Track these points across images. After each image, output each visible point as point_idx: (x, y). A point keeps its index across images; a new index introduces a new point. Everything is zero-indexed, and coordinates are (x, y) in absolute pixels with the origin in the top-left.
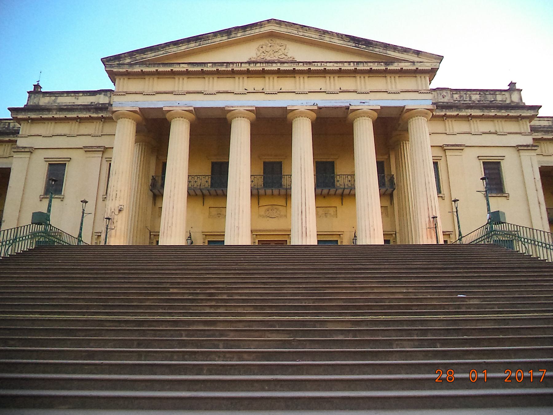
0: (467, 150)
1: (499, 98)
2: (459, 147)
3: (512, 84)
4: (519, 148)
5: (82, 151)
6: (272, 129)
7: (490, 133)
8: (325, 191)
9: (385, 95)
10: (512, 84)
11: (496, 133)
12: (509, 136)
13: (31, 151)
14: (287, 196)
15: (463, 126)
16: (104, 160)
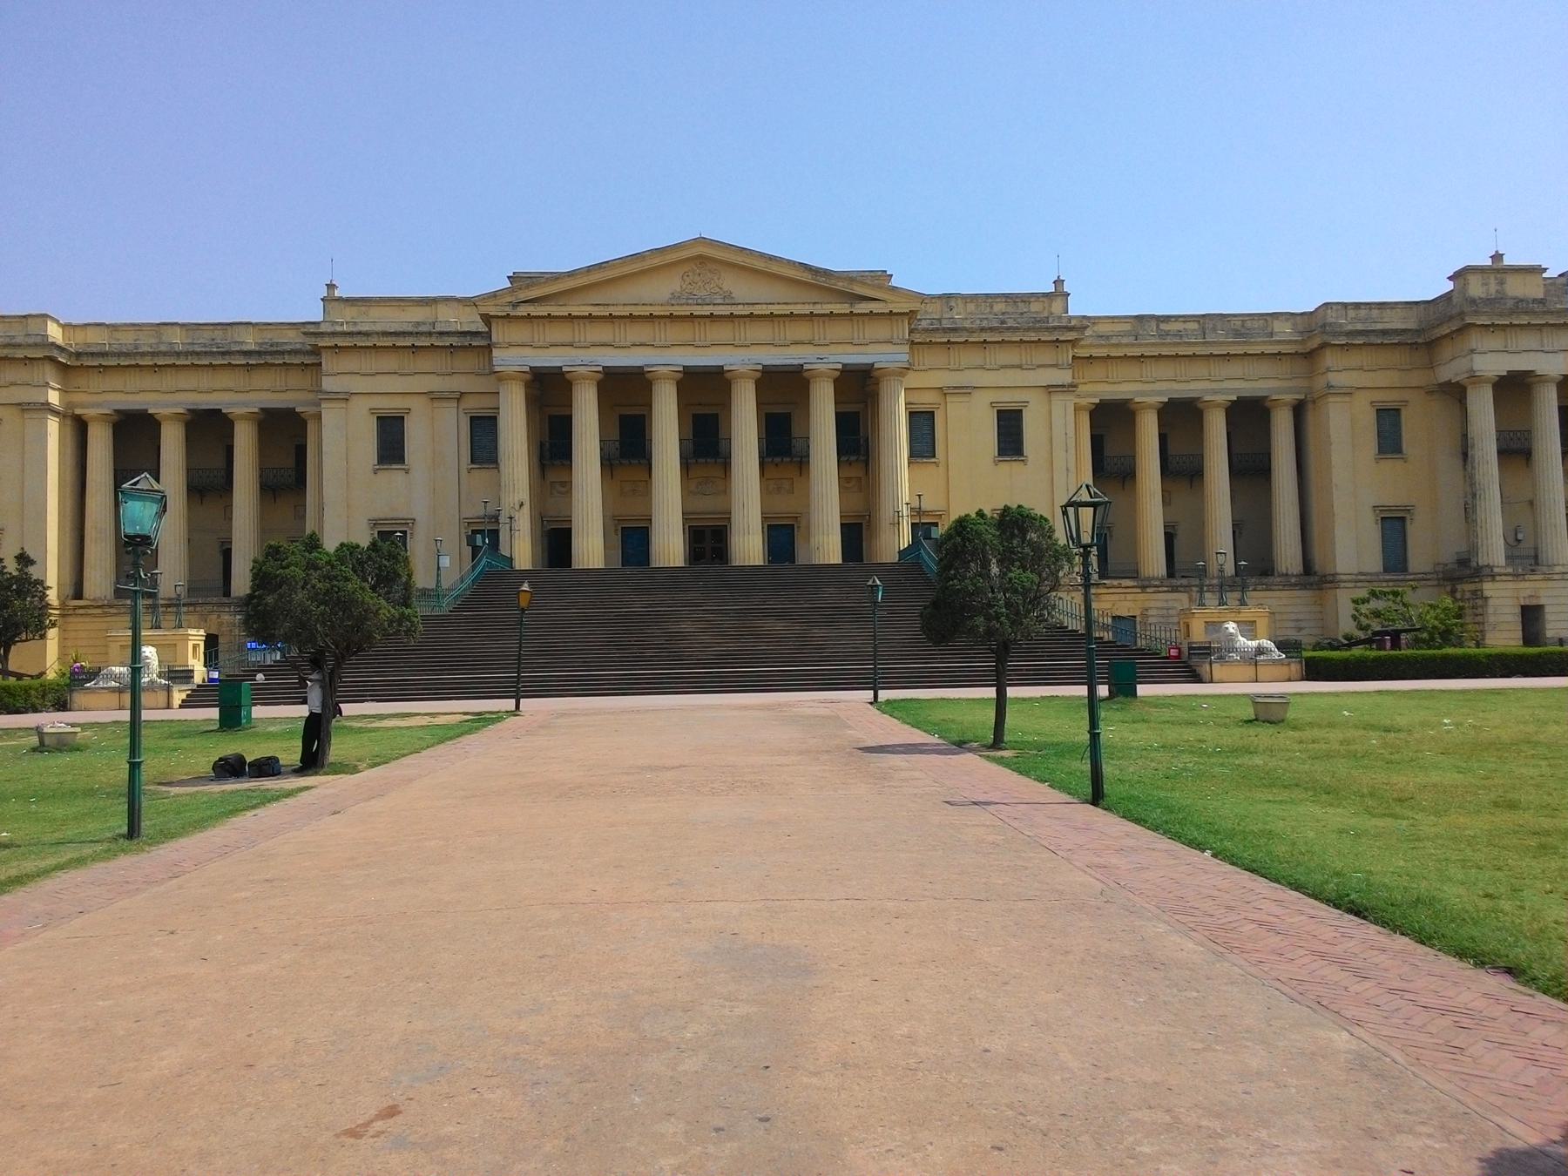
0: (976, 394)
1: (1035, 307)
2: (964, 391)
3: (1058, 282)
4: (1050, 389)
5: (423, 399)
6: (705, 393)
7: (1013, 367)
8: (778, 460)
9: (849, 348)
10: (1058, 282)
11: (1020, 367)
12: (1041, 370)
13: (346, 397)
14: (726, 465)
15: (975, 357)
16: (462, 415)
